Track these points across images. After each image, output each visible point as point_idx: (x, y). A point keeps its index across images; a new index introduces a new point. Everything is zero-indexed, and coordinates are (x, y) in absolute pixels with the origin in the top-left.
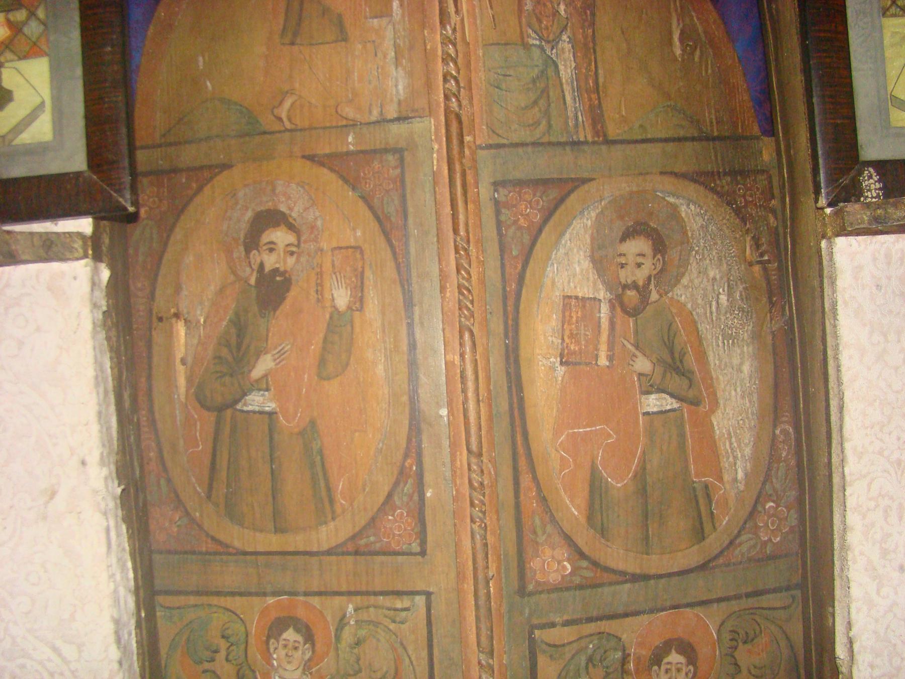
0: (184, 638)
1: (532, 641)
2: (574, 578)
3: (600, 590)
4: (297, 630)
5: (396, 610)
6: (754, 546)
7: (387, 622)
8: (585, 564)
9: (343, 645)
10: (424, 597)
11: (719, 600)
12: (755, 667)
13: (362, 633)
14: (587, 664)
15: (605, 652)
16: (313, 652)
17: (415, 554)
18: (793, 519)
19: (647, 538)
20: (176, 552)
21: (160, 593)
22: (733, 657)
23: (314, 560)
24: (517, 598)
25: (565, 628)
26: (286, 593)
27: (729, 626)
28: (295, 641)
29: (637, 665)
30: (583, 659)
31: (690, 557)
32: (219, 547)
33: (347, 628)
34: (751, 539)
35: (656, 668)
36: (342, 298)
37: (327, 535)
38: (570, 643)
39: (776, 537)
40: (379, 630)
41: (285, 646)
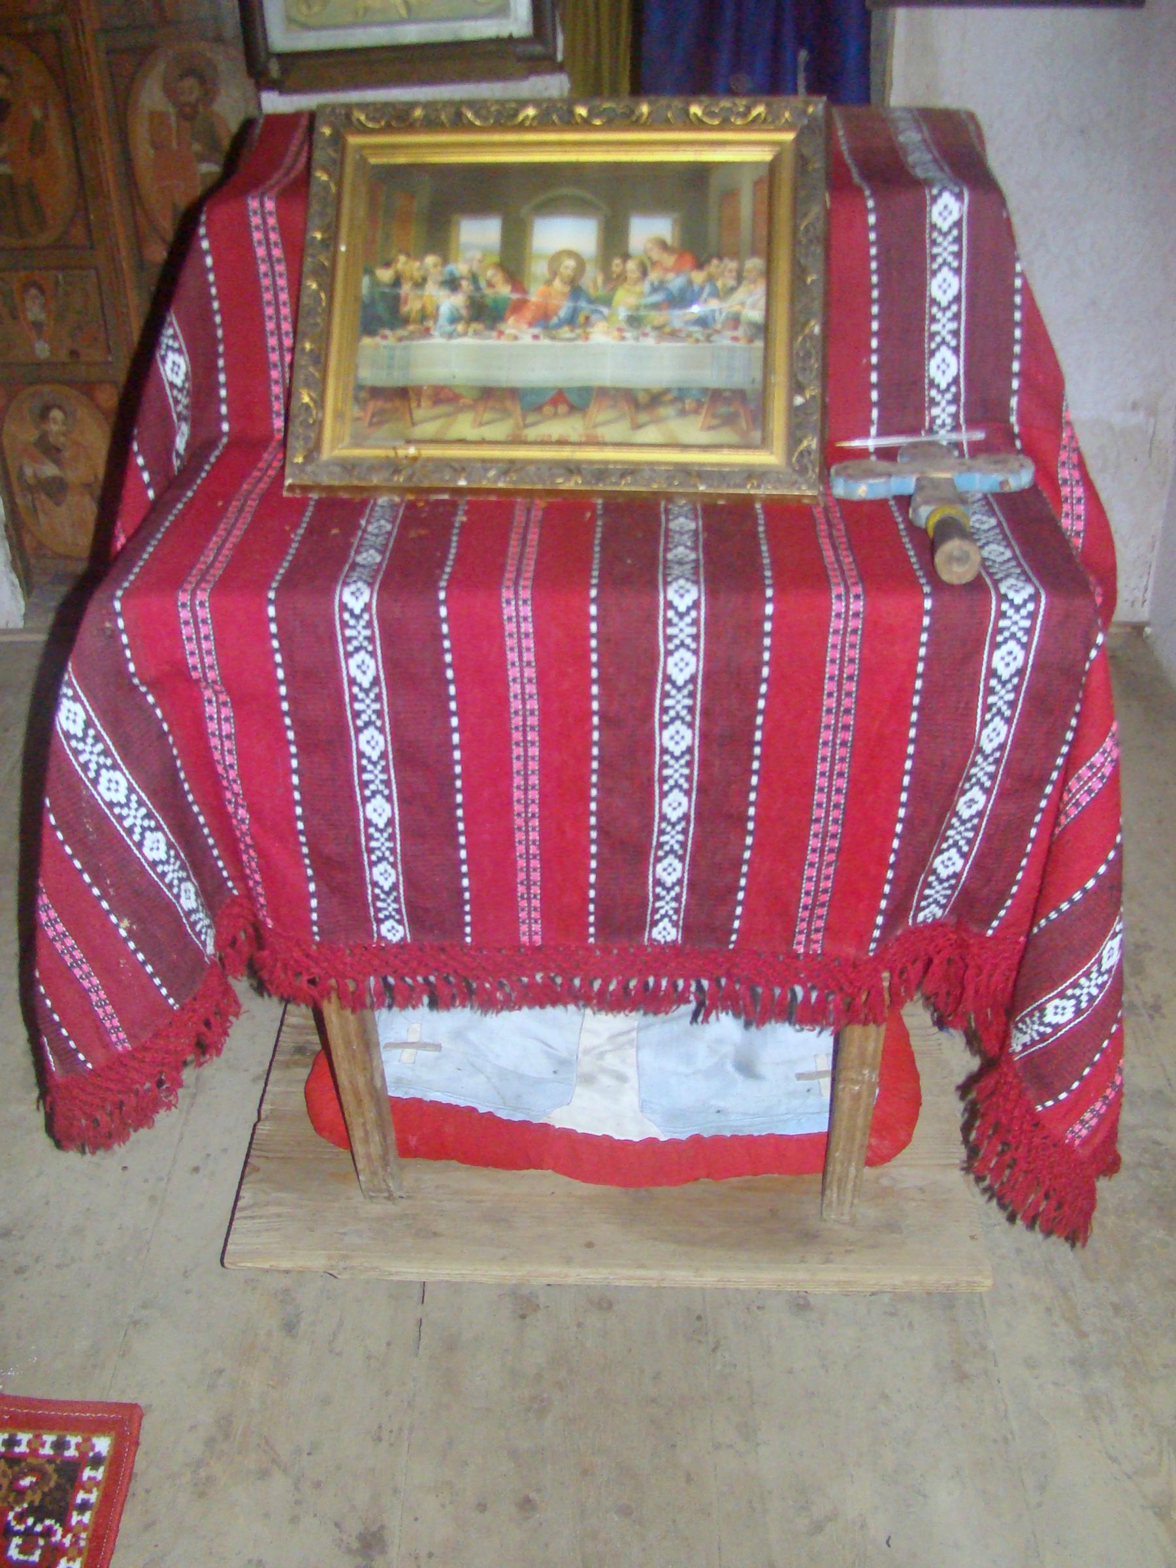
36: (37, 113)
37: (45, 239)
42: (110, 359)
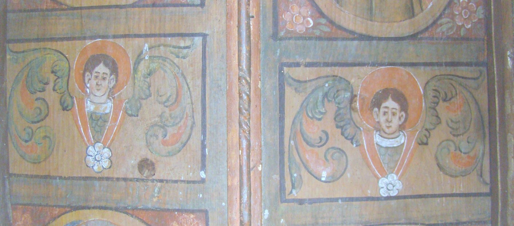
0: (25, 74)
1: (281, 75)
2: (315, 31)
3: (334, 42)
4: (106, 65)
5: (180, 48)
6: (451, 28)
7: (172, 57)
8: (323, 21)
9: (139, 75)
10: (201, 38)
11: (426, 64)
12: (452, 121)
13: (154, 66)
14: (324, 98)
15: (338, 91)
16: (117, 81)
17: (197, 6)
18: (480, 13)
19: (371, 9)
20: (25, 11)
21: (9, 42)
22: (434, 109)
23: (123, 11)
24: (271, 41)
25: (308, 68)
26: (100, 37)
27: (432, 85)
28: (104, 73)
29: (362, 105)
30: (321, 94)
31: (403, 28)
32: (56, 5)
33: (143, 62)
34: (448, 22)
35: (376, 109)
38: (310, 81)
39: (468, 24)
40: (166, 63)
41: (97, 77)
42: (203, 175)
